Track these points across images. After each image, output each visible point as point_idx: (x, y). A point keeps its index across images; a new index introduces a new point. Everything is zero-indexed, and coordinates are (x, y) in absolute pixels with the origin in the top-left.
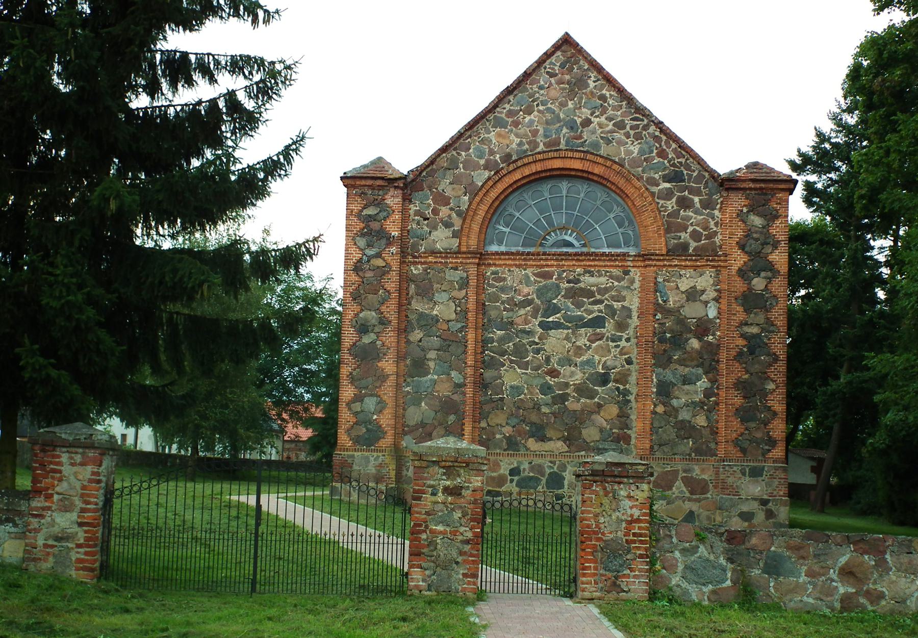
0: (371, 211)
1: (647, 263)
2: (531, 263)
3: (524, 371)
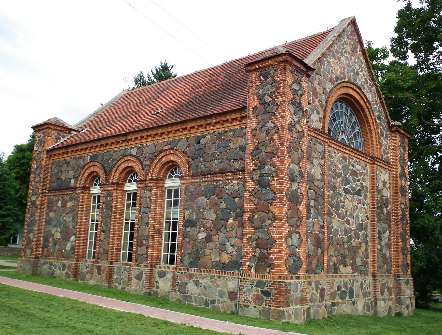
0: (295, 87)
1: (376, 162)
2: (342, 150)
3: (339, 220)
